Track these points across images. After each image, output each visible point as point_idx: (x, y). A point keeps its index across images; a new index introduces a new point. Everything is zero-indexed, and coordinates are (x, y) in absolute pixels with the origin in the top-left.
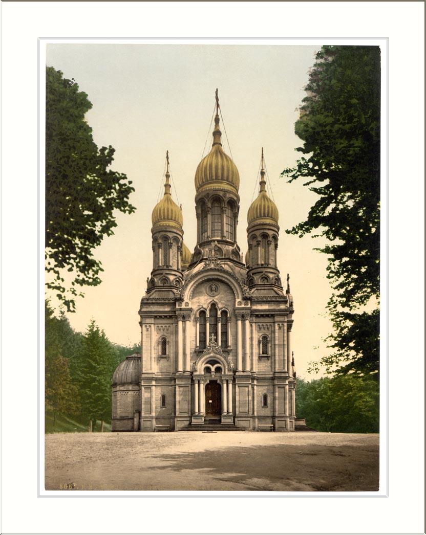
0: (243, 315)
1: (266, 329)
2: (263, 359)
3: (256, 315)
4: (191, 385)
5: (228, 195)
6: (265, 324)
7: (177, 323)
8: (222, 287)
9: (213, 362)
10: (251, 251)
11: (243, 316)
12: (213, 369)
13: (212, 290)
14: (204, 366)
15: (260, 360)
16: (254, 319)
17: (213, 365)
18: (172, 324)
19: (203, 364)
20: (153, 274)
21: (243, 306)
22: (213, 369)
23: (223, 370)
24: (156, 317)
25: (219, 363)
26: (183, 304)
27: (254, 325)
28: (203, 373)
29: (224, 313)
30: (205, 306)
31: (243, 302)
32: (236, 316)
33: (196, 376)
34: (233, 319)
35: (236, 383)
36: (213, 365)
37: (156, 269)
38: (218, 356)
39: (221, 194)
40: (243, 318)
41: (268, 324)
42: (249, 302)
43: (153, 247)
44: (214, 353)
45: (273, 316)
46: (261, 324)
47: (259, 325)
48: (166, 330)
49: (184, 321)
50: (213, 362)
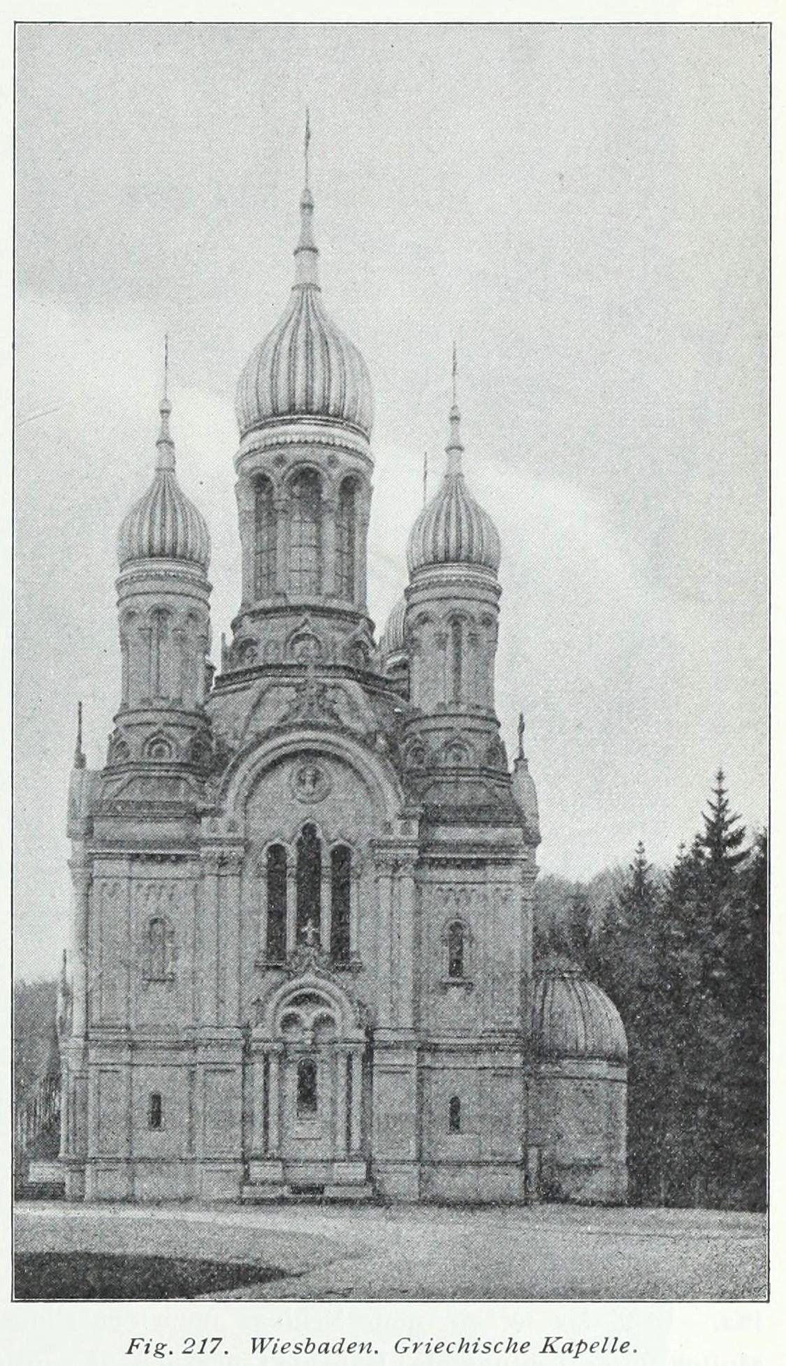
11: (396, 866)
13: (302, 782)
20: (125, 720)
21: (397, 834)
26: (222, 822)
29: (341, 855)
31: (398, 825)
35: (376, 1061)
37: (133, 705)
42: (415, 826)
44: (317, 974)
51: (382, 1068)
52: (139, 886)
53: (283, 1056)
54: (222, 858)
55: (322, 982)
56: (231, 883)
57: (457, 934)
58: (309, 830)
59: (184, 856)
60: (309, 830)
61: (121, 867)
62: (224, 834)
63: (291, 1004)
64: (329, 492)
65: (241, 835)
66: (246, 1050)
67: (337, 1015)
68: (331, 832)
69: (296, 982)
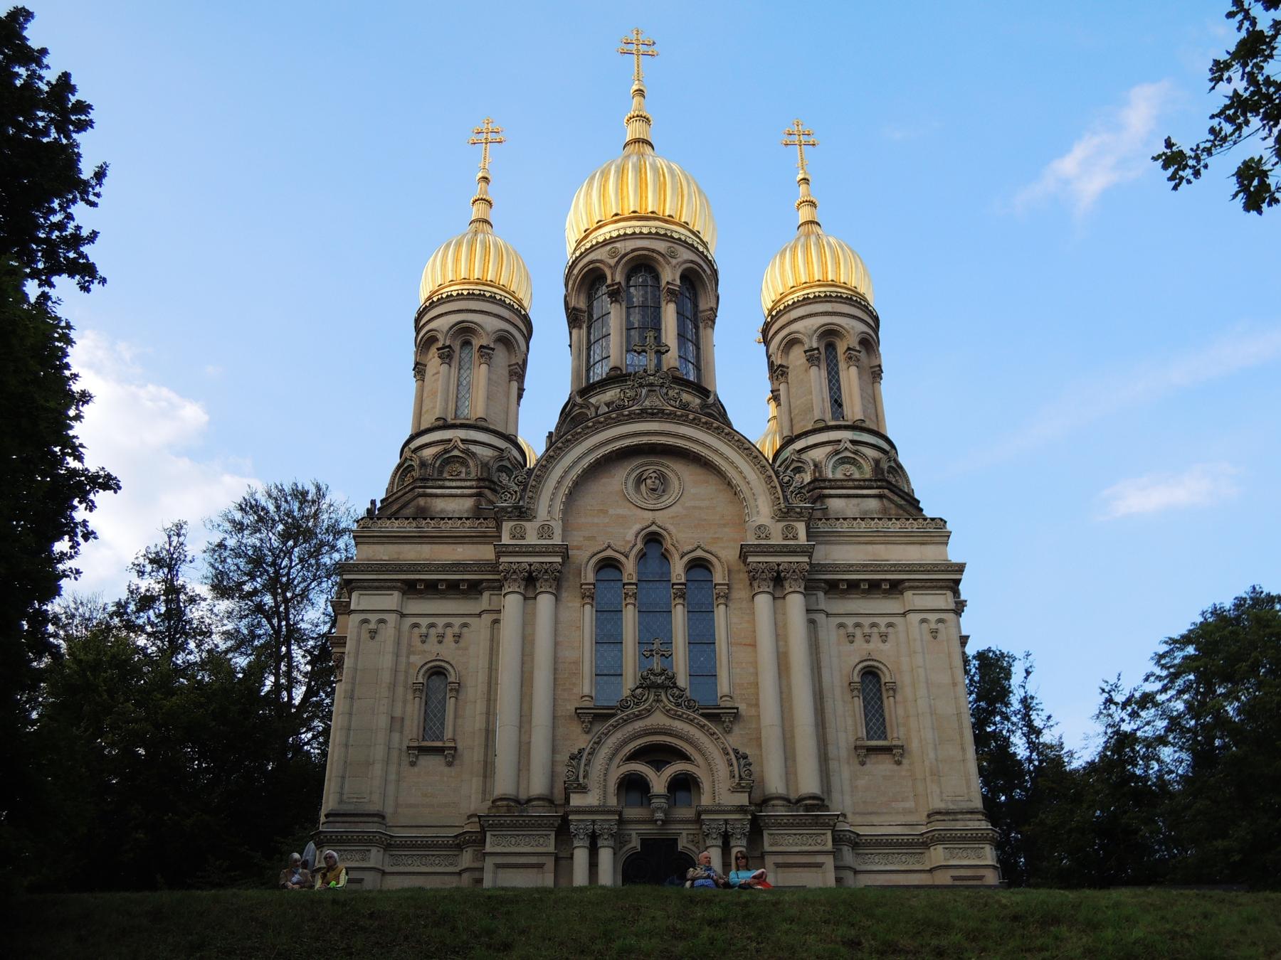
0: (778, 573)
1: (875, 638)
2: (873, 758)
3: (826, 581)
4: (557, 859)
5: (686, 255)
6: (866, 621)
7: (499, 611)
8: (680, 473)
9: (658, 754)
10: (782, 387)
11: (778, 580)
12: (658, 782)
14: (617, 772)
15: (863, 764)
16: (822, 601)
17: (658, 769)
18: (480, 615)
19: (617, 760)
21: (777, 540)
22: (658, 782)
23: (706, 786)
24: (410, 589)
25: (685, 757)
26: (531, 528)
27: (820, 618)
28: (612, 801)
29: (699, 565)
30: (618, 544)
32: (754, 576)
33: (579, 811)
34: (740, 593)
35: (767, 848)
36: (658, 769)
38: (678, 725)
39: (661, 246)
40: (778, 580)
41: (882, 621)
42: (801, 528)
43: (417, 364)
45: (896, 588)
46: (850, 622)
47: (841, 625)
48: (449, 639)
49: (529, 597)
50: (658, 754)
51: (780, 859)
52: (416, 625)
53: (619, 840)
54: (530, 573)
55: (678, 725)
56: (545, 602)
57: (872, 683)
58: (653, 539)
59: (482, 581)
60: (653, 539)
61: (391, 600)
62: (532, 539)
63: (633, 757)
64: (670, 276)
65: (557, 540)
66: (563, 831)
67: (700, 773)
68: (683, 541)
69: (639, 725)
